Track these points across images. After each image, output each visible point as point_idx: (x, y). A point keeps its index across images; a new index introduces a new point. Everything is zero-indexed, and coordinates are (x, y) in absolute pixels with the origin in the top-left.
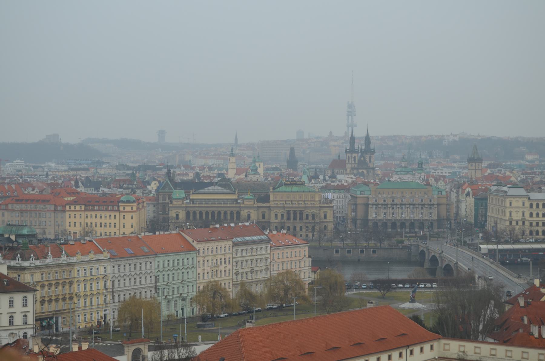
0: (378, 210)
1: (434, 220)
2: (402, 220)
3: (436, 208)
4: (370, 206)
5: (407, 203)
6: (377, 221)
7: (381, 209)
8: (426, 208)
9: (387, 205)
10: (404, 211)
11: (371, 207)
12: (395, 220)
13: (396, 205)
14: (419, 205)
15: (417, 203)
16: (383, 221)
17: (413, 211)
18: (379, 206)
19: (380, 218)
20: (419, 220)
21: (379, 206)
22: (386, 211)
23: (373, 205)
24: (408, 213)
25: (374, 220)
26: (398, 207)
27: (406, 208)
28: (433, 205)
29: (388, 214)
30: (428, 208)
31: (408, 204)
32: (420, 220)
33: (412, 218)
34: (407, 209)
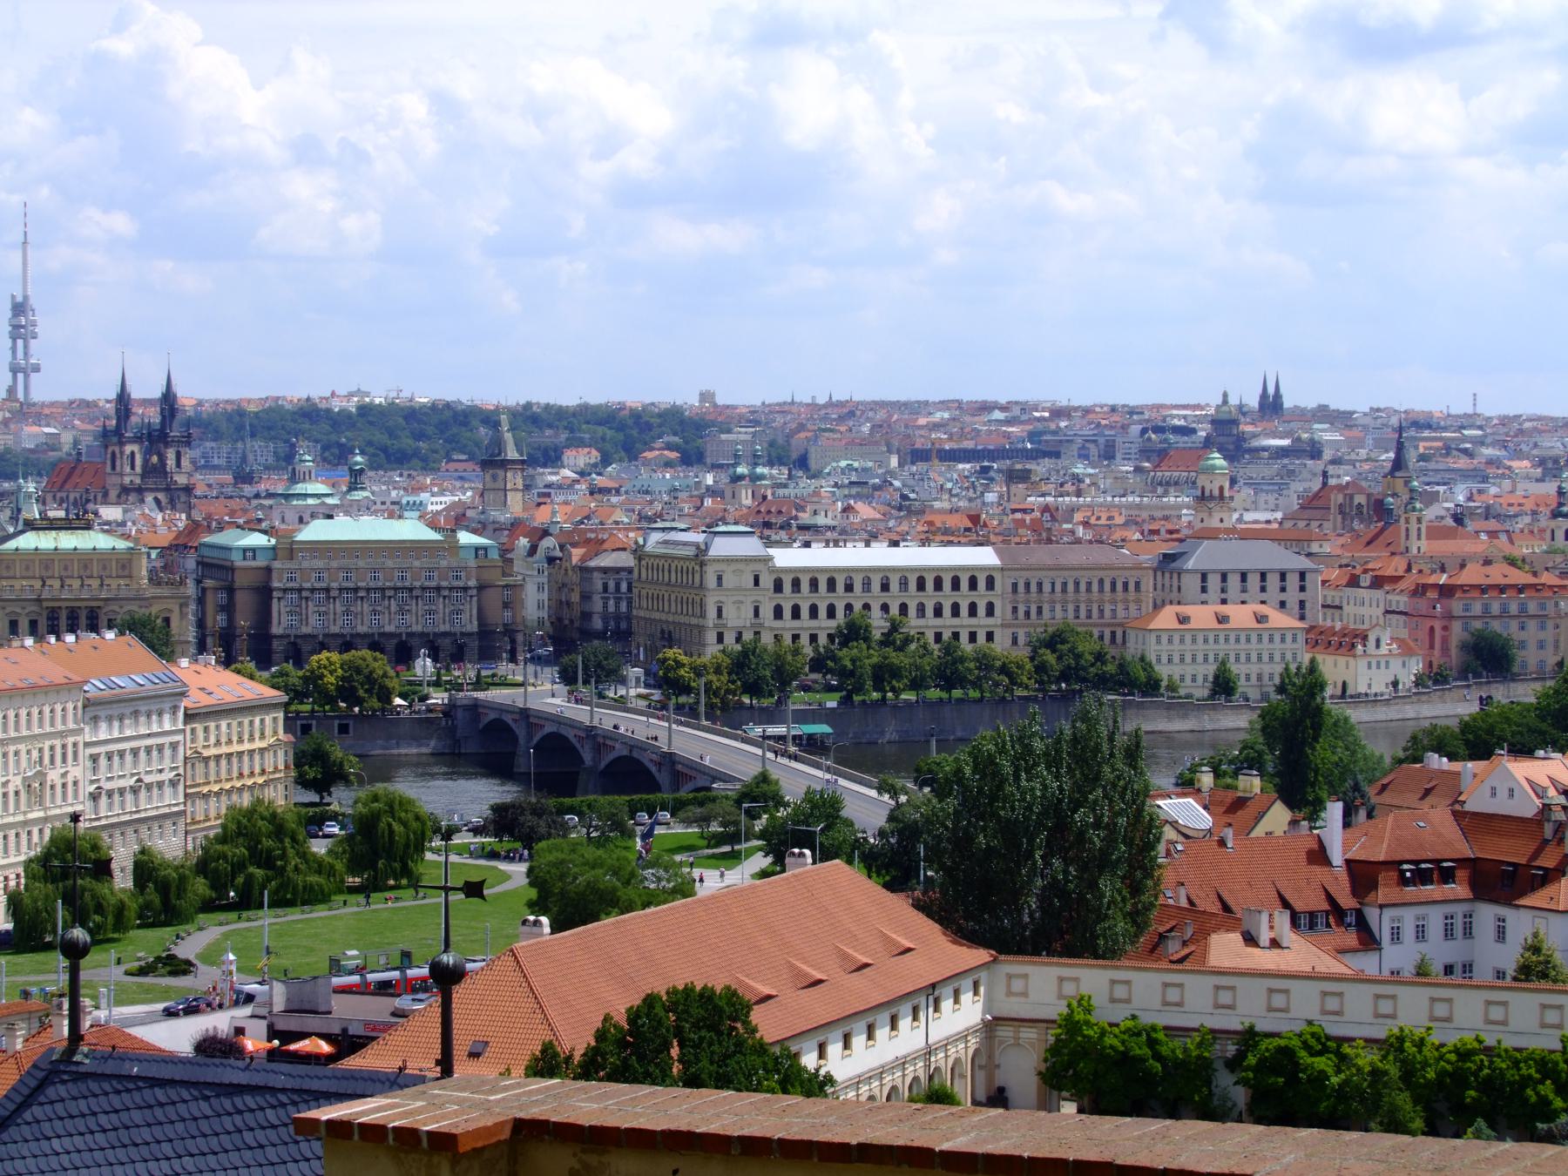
0: (300, 606)
1: (470, 634)
2: (373, 634)
3: (475, 599)
4: (275, 594)
5: (388, 584)
6: (299, 641)
8: (444, 597)
9: (327, 590)
10: (379, 608)
11: (279, 599)
12: (352, 635)
13: (356, 590)
14: (424, 589)
15: (417, 584)
17: (407, 608)
18: (305, 594)
19: (305, 630)
21: (305, 594)
22: (324, 609)
23: (285, 590)
25: (289, 636)
26: (362, 598)
27: (383, 599)
28: (465, 589)
29: (332, 617)
30: (449, 597)
31: (390, 588)
32: (428, 634)
33: (403, 630)
34: (387, 602)
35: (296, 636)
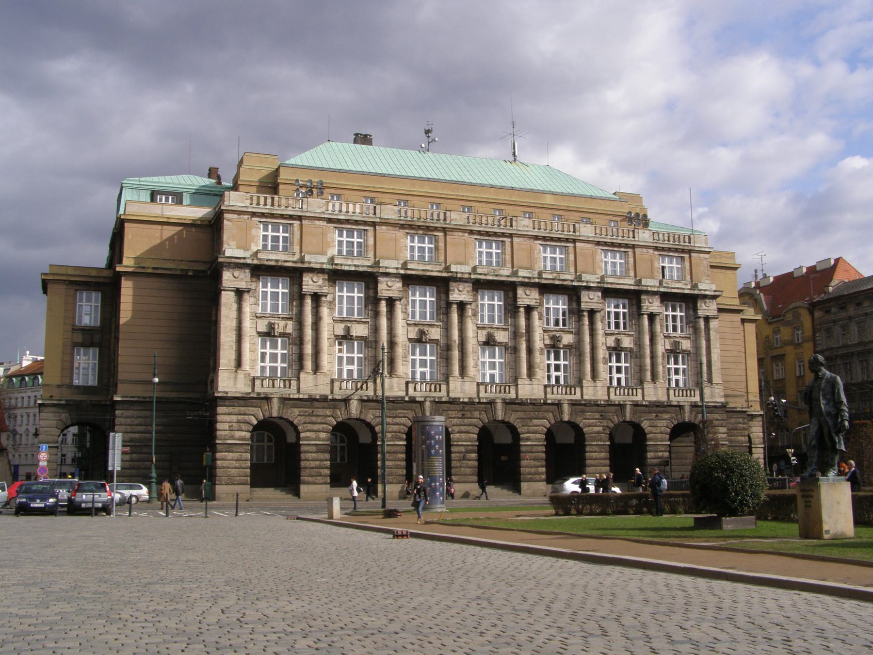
2: (491, 403)
5: (522, 273)
6: (294, 414)
7: (325, 311)
16: (341, 415)
20: (609, 404)
23: (259, 271)
24: (530, 351)
25: (267, 399)
35: (284, 400)
